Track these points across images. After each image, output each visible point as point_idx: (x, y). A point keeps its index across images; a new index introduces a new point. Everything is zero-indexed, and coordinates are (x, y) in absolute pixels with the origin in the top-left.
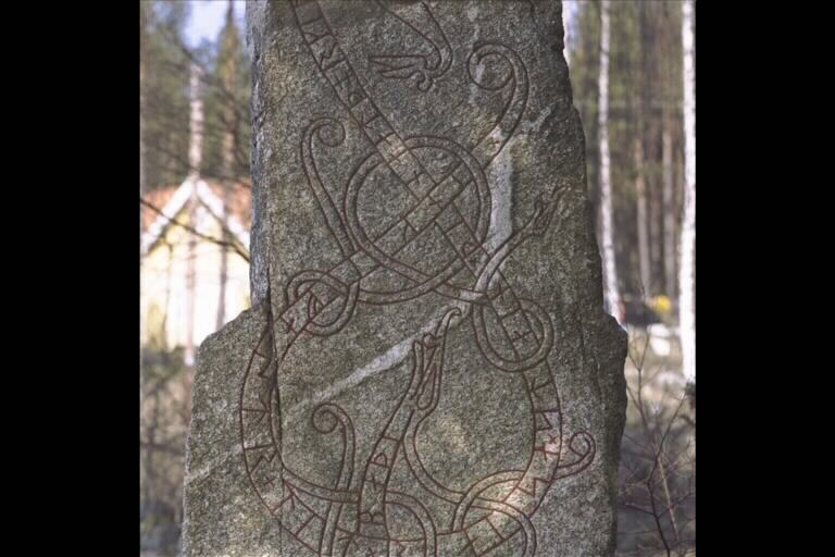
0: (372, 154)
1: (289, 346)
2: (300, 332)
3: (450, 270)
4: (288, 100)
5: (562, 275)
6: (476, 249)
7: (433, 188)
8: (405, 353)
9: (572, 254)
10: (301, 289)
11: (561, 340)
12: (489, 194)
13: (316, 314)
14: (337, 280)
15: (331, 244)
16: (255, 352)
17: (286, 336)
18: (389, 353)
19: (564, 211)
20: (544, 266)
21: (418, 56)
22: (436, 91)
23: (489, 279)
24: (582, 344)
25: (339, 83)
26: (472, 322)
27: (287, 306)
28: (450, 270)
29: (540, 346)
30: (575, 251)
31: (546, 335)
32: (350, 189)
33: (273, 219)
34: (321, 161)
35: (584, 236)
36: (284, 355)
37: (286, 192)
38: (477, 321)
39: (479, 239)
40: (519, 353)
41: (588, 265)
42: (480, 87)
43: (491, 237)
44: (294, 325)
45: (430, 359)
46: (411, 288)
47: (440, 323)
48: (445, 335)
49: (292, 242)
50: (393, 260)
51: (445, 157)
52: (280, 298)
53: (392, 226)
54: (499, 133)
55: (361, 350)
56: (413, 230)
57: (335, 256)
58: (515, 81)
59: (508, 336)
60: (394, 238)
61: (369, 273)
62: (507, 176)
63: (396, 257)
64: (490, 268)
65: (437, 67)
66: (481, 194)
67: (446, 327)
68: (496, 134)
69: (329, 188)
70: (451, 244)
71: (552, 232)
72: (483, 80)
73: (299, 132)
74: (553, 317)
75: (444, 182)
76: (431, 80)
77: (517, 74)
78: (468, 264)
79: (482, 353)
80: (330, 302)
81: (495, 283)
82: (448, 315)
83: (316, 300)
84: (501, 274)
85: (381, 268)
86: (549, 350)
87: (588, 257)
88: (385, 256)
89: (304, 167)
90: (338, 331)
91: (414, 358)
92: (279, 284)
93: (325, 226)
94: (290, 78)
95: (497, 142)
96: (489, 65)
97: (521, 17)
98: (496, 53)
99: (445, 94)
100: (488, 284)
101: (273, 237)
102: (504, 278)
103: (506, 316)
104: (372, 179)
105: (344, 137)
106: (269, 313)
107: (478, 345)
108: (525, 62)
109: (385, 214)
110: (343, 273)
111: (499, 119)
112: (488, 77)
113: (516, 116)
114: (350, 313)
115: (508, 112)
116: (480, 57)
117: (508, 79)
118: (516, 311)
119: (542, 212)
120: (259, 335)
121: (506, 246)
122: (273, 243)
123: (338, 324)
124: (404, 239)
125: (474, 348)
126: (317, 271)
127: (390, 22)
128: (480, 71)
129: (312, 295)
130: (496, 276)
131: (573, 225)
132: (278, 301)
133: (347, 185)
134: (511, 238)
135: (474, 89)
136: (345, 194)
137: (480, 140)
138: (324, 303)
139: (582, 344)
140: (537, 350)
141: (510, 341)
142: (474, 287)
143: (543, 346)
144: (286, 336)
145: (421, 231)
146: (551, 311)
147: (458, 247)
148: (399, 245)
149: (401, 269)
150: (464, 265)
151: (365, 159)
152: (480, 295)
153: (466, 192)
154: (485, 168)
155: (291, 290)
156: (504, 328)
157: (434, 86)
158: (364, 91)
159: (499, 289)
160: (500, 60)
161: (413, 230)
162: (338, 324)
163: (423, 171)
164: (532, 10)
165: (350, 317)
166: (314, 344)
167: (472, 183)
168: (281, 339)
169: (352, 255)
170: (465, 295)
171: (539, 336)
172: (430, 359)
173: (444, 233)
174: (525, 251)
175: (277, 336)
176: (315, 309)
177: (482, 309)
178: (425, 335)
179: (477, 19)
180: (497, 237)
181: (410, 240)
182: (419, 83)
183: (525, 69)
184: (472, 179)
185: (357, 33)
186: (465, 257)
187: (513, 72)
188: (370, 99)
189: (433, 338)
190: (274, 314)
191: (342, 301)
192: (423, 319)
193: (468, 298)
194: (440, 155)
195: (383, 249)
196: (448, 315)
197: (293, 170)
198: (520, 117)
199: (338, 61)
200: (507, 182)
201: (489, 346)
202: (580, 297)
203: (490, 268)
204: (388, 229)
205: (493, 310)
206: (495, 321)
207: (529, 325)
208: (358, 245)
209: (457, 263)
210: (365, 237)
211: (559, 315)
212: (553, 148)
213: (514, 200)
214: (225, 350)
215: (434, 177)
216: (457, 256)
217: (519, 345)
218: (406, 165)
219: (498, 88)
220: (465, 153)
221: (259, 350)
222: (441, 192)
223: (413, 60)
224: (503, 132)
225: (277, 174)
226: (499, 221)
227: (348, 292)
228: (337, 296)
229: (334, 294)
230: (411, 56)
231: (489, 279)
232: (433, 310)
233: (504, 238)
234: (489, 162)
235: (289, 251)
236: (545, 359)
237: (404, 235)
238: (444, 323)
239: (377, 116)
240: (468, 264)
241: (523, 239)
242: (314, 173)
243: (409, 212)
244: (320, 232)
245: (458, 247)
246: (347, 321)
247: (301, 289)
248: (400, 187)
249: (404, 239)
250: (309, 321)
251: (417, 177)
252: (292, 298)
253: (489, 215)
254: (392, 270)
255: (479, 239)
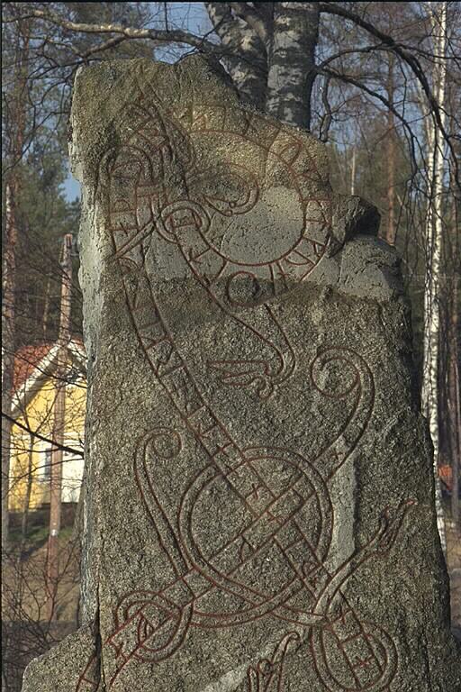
0: (208, 465)
1: (118, 671)
2: (130, 657)
3: (288, 590)
4: (123, 409)
5: (407, 596)
6: (316, 567)
7: (273, 502)
8: (239, 679)
9: (417, 573)
10: (132, 611)
11: (405, 666)
12: (331, 509)
13: (146, 637)
14: (169, 602)
15: (164, 563)
16: (82, 677)
17: (115, 661)
18: (222, 679)
19: (410, 527)
20: (388, 586)
21: (259, 362)
22: (278, 398)
23: (329, 601)
24: (427, 671)
25: (175, 390)
26: (311, 647)
27: (117, 628)
28: (288, 590)
29: (382, 674)
30: (421, 570)
31: (389, 661)
32: (184, 503)
33: (104, 536)
34: (155, 473)
35: (431, 555)
36: (112, 680)
37: (118, 507)
38: (316, 646)
39: (320, 558)
40: (360, 680)
41: (435, 586)
42: (323, 394)
43: (331, 556)
44: (123, 650)
45: (266, 687)
46: (247, 610)
47: (276, 650)
48: (282, 661)
49: (123, 560)
50: (227, 580)
51: (284, 469)
52: (109, 620)
53: (228, 544)
54: (342, 443)
55: (194, 676)
56: (250, 547)
57: (166, 575)
58: (360, 388)
59: (348, 663)
60: (228, 555)
61: (203, 594)
62: (351, 489)
63: (231, 577)
64: (330, 589)
65: (278, 372)
66: (323, 509)
67: (283, 653)
68: (339, 444)
69: (163, 503)
70: (290, 563)
71: (397, 550)
72: (326, 388)
73: (133, 442)
74: (397, 642)
75: (284, 497)
76: (272, 386)
77: (362, 380)
78: (307, 584)
79: (321, 681)
80: (160, 625)
81: (335, 606)
82: (285, 639)
83: (147, 622)
84: (343, 596)
85: (215, 589)
86: (392, 677)
87: (435, 576)
88: (220, 576)
89: (136, 479)
90: (169, 655)
91: (249, 684)
92: (109, 605)
93: (157, 544)
94: (125, 385)
95: (341, 453)
96: (333, 370)
97: (367, 320)
98: (341, 358)
99: (286, 401)
100: (328, 606)
101: (103, 555)
102: (345, 600)
103: (346, 640)
104: (208, 492)
105: (180, 448)
106: (98, 636)
107: (317, 671)
108: (371, 368)
109: (221, 530)
110: (175, 595)
111: (343, 428)
112: (333, 383)
113: (361, 426)
114: (182, 637)
115: (352, 421)
116: (324, 362)
117: (353, 386)
118: (357, 634)
119: (387, 526)
120: (87, 660)
121: (348, 565)
122: (103, 562)
123: (170, 648)
124: (240, 557)
125: (313, 674)
126: (150, 592)
127: (230, 326)
128: (323, 378)
129: (143, 617)
130: (337, 596)
131: (419, 543)
132: (106, 624)
133: (182, 499)
134: (353, 556)
135: (316, 396)
136: (179, 508)
137: (322, 451)
138: (155, 626)
139: (427, 671)
140: (379, 677)
141: (351, 668)
142: (313, 609)
143: (386, 673)
144: (115, 661)
145: (258, 548)
146: (395, 635)
147: (298, 567)
148: (235, 564)
149: (236, 590)
150: (303, 584)
151: (201, 471)
152: (321, 618)
153: (307, 506)
154: (327, 481)
155: (120, 612)
156: (344, 653)
157: (275, 392)
158: (201, 399)
159: (339, 611)
160: (344, 366)
161: (250, 547)
162: (170, 648)
163: (262, 484)
164: (380, 312)
165: (182, 641)
166: (144, 669)
167: (314, 497)
168: (109, 664)
169: (185, 575)
170: (303, 617)
171: (381, 662)
172: (266, 687)
173: (283, 551)
174: (368, 571)
175: (105, 660)
176: (145, 633)
177: (321, 632)
178: (260, 662)
179: (321, 322)
180: (338, 555)
181: (248, 558)
182: (258, 390)
183: (371, 376)
184: (313, 491)
185: (196, 337)
186: (305, 576)
187: (358, 376)
188: (208, 408)
189: (269, 664)
190: (103, 637)
191: (174, 623)
192: (258, 644)
193: (307, 621)
194: (280, 468)
195: (218, 568)
196: (285, 639)
197: (125, 484)
198: (365, 426)
199: (174, 368)
200: (350, 496)
201: (328, 672)
202: (426, 620)
203: (330, 589)
204: (224, 547)
205: (333, 634)
206: (335, 646)
207: (371, 650)
208: (192, 564)
209: (296, 583)
210: (199, 556)
211: (404, 641)
212: (400, 459)
213: (357, 516)
214: (51, 674)
215: (273, 491)
216: (296, 576)
217: (360, 672)
218: (244, 478)
219: (342, 395)
220: (306, 464)
221: (86, 676)
222: (280, 506)
223: (254, 366)
224: (347, 442)
225: (109, 488)
226: (340, 533)
227: (181, 613)
228: (169, 619)
229: (166, 615)
230: (252, 361)
231: (329, 601)
232: (269, 633)
233: (346, 558)
234: (331, 474)
235: (120, 570)
236: (387, 686)
237: (240, 553)
238: (281, 648)
239: (215, 425)
240: (307, 584)
241: (366, 557)
242: (147, 487)
243: (246, 528)
244: (152, 549)
245: (298, 567)
246: (179, 644)
247: (132, 611)
248: (238, 502)
249: (240, 557)
250: (139, 645)
251: (255, 490)
252: (121, 620)
253: (331, 532)
254: (227, 591)
255: (320, 558)
